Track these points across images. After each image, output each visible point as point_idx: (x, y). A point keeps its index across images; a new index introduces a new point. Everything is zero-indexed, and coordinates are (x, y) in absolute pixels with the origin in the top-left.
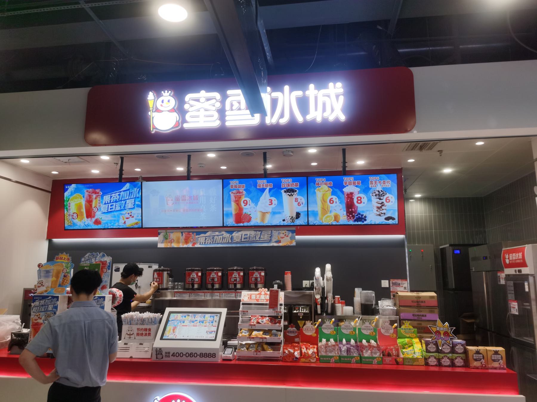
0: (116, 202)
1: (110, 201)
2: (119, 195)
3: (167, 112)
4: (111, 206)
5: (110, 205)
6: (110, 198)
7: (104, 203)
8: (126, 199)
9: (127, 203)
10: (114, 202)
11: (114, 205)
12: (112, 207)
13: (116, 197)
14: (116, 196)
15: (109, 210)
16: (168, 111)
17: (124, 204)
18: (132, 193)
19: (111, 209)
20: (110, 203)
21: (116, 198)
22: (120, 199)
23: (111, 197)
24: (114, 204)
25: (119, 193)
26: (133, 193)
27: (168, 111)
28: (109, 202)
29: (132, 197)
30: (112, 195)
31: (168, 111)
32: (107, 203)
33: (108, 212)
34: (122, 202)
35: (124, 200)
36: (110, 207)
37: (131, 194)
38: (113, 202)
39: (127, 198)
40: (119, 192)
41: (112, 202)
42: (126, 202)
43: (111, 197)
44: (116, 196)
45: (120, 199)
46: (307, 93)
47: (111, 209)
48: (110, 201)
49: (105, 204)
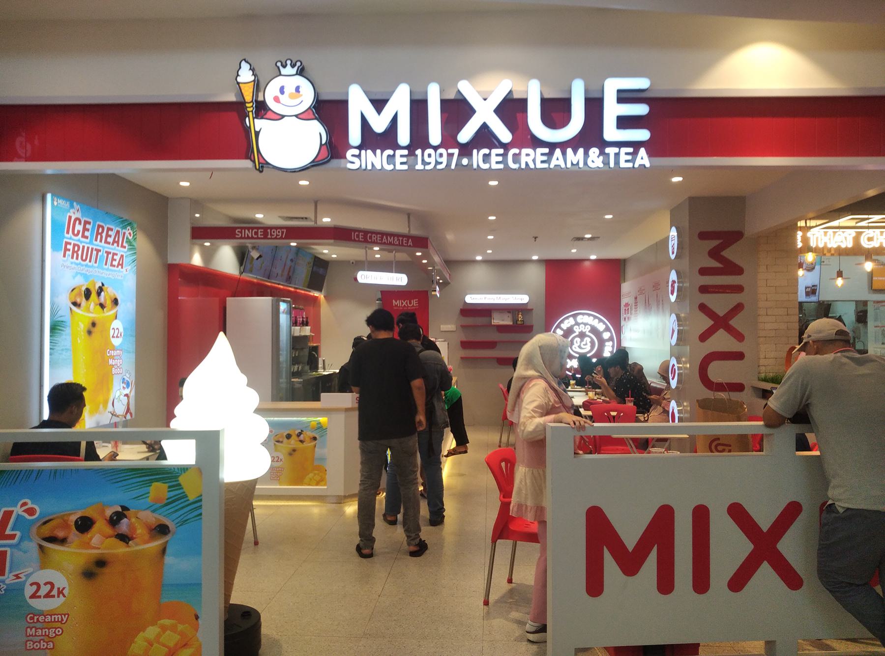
3: (294, 117)
16: (297, 116)
27: (297, 116)
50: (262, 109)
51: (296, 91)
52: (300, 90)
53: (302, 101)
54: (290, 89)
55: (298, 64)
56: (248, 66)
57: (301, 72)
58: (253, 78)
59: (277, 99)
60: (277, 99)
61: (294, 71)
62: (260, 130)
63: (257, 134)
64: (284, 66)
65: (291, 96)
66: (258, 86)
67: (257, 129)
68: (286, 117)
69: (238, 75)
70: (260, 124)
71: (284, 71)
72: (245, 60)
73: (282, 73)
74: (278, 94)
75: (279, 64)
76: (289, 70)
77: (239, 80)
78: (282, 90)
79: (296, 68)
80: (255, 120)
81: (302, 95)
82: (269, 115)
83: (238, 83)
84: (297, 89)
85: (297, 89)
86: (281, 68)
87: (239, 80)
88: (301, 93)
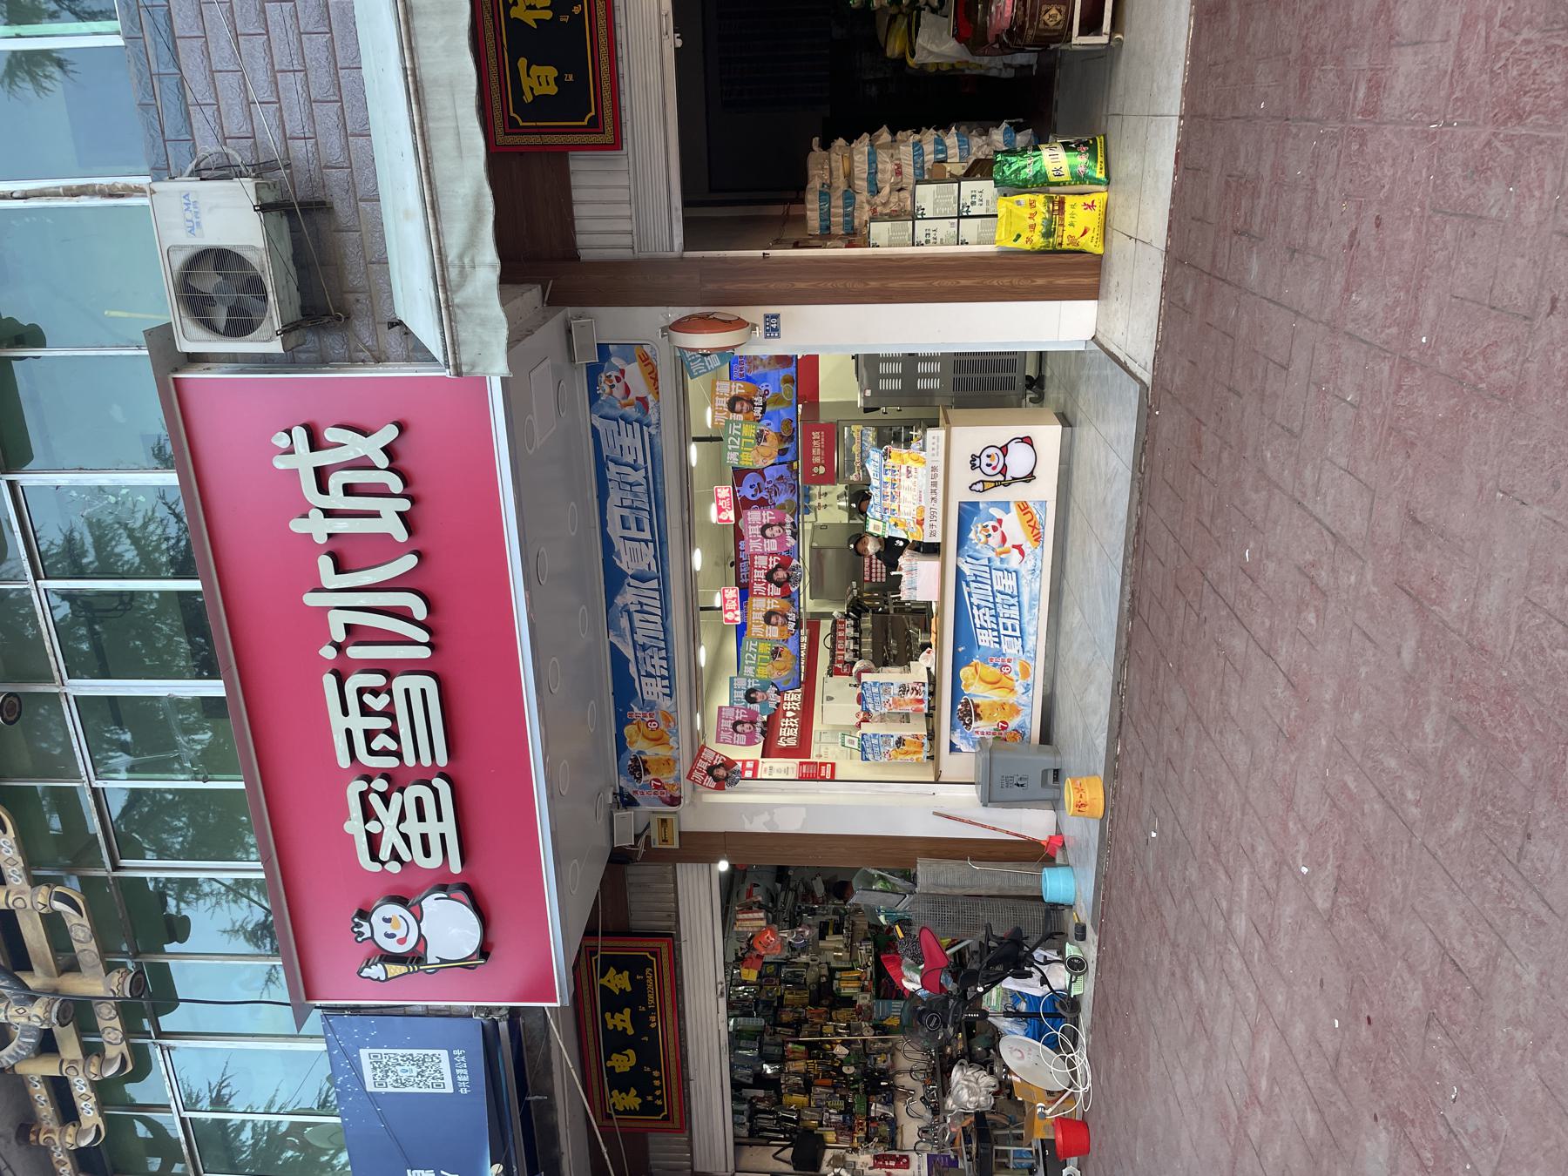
0: (996, 616)
1: (993, 630)
2: (979, 607)
4: (1006, 629)
5: (1002, 632)
6: (985, 631)
7: (997, 646)
8: (992, 591)
9: (1002, 589)
10: (997, 620)
11: (1005, 620)
12: (1010, 628)
13: (984, 615)
14: (981, 616)
15: (1018, 634)
17: (1003, 597)
18: (976, 576)
19: (1014, 630)
20: (998, 631)
21: (987, 614)
22: (992, 606)
23: (982, 628)
24: (1001, 621)
25: (975, 608)
26: (977, 573)
28: (996, 633)
29: (988, 576)
30: (978, 626)
32: (999, 637)
33: (1022, 637)
34: (997, 600)
35: (994, 596)
36: (1010, 632)
37: (979, 579)
38: (997, 624)
39: (990, 589)
40: (972, 609)
41: (995, 627)
42: (999, 592)
43: (982, 628)
44: (981, 616)
45: (992, 606)
47: (1014, 630)
48: (993, 630)
49: (1000, 643)
50: (415, 958)
54: (389, 928)
55: (356, 920)
56: (366, 970)
57: (364, 914)
59: (402, 941)
60: (402, 941)
61: (366, 924)
63: (443, 961)
66: (389, 958)
69: (378, 979)
72: (359, 973)
73: (368, 934)
74: (396, 939)
75: (359, 939)
77: (383, 978)
78: (391, 936)
82: (420, 949)
83: (387, 979)
87: (383, 978)
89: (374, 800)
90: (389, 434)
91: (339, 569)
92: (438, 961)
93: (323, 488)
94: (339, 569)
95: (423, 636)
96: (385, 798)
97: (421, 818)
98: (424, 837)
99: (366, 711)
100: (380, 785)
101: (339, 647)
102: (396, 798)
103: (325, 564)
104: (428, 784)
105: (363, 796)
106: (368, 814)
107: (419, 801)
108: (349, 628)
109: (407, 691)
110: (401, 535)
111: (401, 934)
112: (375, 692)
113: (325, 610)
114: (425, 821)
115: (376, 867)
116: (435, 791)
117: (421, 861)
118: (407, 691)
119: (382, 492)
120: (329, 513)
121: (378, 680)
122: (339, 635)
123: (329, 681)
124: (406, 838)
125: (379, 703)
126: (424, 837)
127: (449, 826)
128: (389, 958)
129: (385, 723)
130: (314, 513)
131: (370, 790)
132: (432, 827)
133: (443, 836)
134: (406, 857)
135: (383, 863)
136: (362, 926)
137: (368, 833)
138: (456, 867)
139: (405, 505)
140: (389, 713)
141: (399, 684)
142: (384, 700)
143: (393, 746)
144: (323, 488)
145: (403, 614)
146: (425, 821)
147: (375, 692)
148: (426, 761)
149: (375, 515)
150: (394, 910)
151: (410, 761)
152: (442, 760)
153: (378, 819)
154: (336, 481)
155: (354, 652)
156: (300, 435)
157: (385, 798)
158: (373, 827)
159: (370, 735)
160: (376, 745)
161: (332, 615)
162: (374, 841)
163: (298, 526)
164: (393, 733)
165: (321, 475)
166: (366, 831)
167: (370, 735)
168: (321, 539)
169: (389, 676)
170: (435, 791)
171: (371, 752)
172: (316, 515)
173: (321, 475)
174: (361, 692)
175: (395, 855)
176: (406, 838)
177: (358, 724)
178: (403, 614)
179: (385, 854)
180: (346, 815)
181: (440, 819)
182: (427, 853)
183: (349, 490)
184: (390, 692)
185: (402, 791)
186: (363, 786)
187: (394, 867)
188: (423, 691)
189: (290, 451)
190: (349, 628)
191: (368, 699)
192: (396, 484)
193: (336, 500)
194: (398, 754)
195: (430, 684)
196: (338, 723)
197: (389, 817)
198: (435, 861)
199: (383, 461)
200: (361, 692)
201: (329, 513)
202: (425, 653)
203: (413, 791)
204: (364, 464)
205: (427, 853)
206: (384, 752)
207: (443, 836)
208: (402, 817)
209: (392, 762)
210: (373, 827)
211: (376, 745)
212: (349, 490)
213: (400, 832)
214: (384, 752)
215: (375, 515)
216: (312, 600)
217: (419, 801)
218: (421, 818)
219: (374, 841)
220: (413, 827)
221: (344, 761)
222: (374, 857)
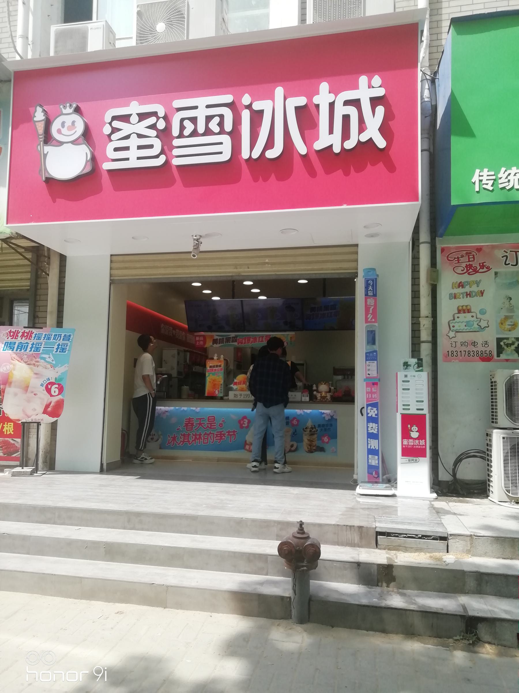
31: (74, 142)
46: (316, 100)
50: (48, 138)
51: (72, 125)
52: (75, 123)
53: (76, 131)
54: (68, 123)
58: (44, 117)
59: (59, 131)
60: (59, 131)
61: (70, 111)
62: (48, 152)
63: (45, 156)
64: (65, 107)
65: (69, 129)
66: (48, 123)
67: (45, 153)
68: (65, 145)
70: (47, 149)
71: (64, 111)
73: (64, 111)
74: (60, 127)
76: (69, 110)
79: (72, 109)
80: (45, 147)
81: (76, 127)
84: (73, 123)
85: (73, 123)
86: (63, 109)
87: (35, 119)
88: (76, 126)
89: (152, 120)
90: (381, 143)
91: (298, 109)
92: (45, 153)
93: (347, 103)
94: (298, 109)
95: (256, 155)
96: (153, 127)
97: (140, 147)
98: (127, 148)
99: (209, 118)
100: (161, 125)
101: (249, 107)
102: (154, 133)
103: (302, 101)
104: (162, 152)
105: (155, 114)
106: (142, 117)
107: (151, 146)
108: (261, 113)
109: (221, 143)
110: (319, 145)
111: (64, 131)
112: (221, 124)
113: (273, 100)
114: (138, 149)
115: (108, 119)
116: (157, 157)
117: (111, 146)
118: (221, 143)
119: (346, 135)
120: (332, 105)
121: (228, 126)
122: (257, 106)
123: (228, 98)
124: (127, 137)
125: (214, 126)
126: (127, 148)
127: (134, 164)
128: (48, 123)
129: (201, 129)
130: (332, 96)
131: (158, 118)
132: (133, 154)
133: (127, 159)
134: (114, 137)
135: (110, 124)
136: (70, 108)
137: (130, 115)
138: (107, 166)
139: (337, 149)
140: (208, 132)
141: (226, 139)
142: (217, 129)
143: (186, 132)
144: (347, 103)
145: (270, 144)
146: (138, 149)
147: (221, 124)
148: (175, 152)
149: (331, 132)
150: (80, 128)
151: (176, 142)
152: (176, 162)
153: (139, 121)
154: (352, 111)
155: (246, 115)
156: (381, 92)
157: (153, 127)
158: (134, 119)
159: (194, 120)
160: (187, 123)
161: (269, 102)
162: (125, 118)
163: (324, 87)
164: (194, 134)
165: (356, 103)
166: (131, 115)
167: (194, 120)
168: (316, 100)
169: (229, 134)
170: (157, 157)
171: (182, 120)
172: (331, 98)
173: (356, 103)
174: (221, 117)
175: (115, 130)
176: (127, 137)
177: (201, 114)
178: (270, 144)
179: (116, 124)
180: (141, 103)
181: (139, 158)
182: (116, 149)
183: (346, 118)
184: (219, 133)
185: (157, 137)
186: (161, 114)
187: (107, 130)
188: (221, 153)
189: (370, 86)
190: (261, 113)
191: (217, 120)
192: (350, 144)
193: (340, 111)
194: (181, 136)
195: (226, 156)
196: (202, 101)
197: (142, 127)
198: (111, 153)
199: (364, 138)
200: (221, 117)
201: (332, 105)
202: (245, 154)
203: (158, 144)
204: (362, 128)
205: (116, 149)
206: (182, 128)
207: (127, 159)
208: (140, 136)
209: (175, 131)
210: (134, 119)
211: (187, 123)
212: (346, 118)
213: (130, 135)
214: (182, 128)
215: (331, 132)
216: (279, 92)
217: (151, 146)
218: (140, 147)
219: (125, 118)
220: (134, 142)
221: (177, 103)
222: (114, 118)
